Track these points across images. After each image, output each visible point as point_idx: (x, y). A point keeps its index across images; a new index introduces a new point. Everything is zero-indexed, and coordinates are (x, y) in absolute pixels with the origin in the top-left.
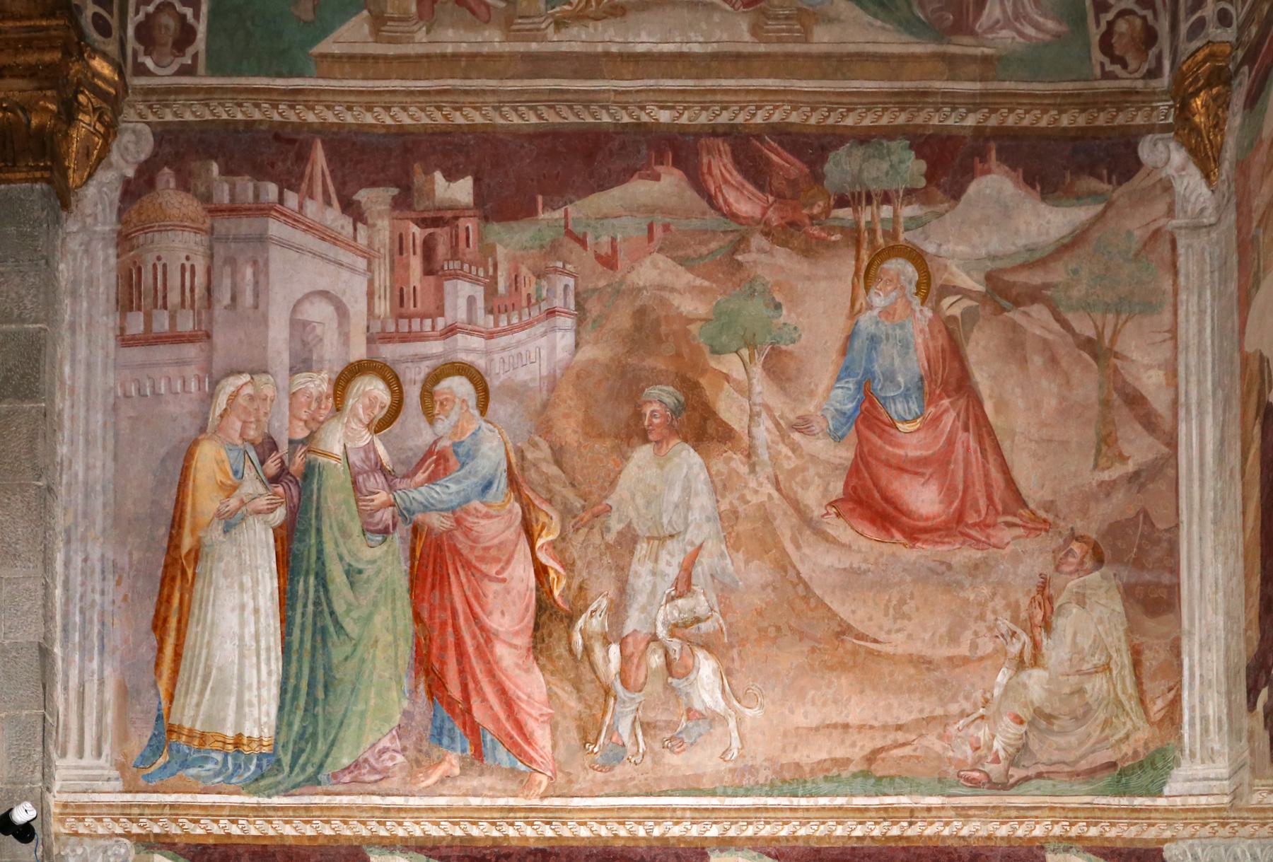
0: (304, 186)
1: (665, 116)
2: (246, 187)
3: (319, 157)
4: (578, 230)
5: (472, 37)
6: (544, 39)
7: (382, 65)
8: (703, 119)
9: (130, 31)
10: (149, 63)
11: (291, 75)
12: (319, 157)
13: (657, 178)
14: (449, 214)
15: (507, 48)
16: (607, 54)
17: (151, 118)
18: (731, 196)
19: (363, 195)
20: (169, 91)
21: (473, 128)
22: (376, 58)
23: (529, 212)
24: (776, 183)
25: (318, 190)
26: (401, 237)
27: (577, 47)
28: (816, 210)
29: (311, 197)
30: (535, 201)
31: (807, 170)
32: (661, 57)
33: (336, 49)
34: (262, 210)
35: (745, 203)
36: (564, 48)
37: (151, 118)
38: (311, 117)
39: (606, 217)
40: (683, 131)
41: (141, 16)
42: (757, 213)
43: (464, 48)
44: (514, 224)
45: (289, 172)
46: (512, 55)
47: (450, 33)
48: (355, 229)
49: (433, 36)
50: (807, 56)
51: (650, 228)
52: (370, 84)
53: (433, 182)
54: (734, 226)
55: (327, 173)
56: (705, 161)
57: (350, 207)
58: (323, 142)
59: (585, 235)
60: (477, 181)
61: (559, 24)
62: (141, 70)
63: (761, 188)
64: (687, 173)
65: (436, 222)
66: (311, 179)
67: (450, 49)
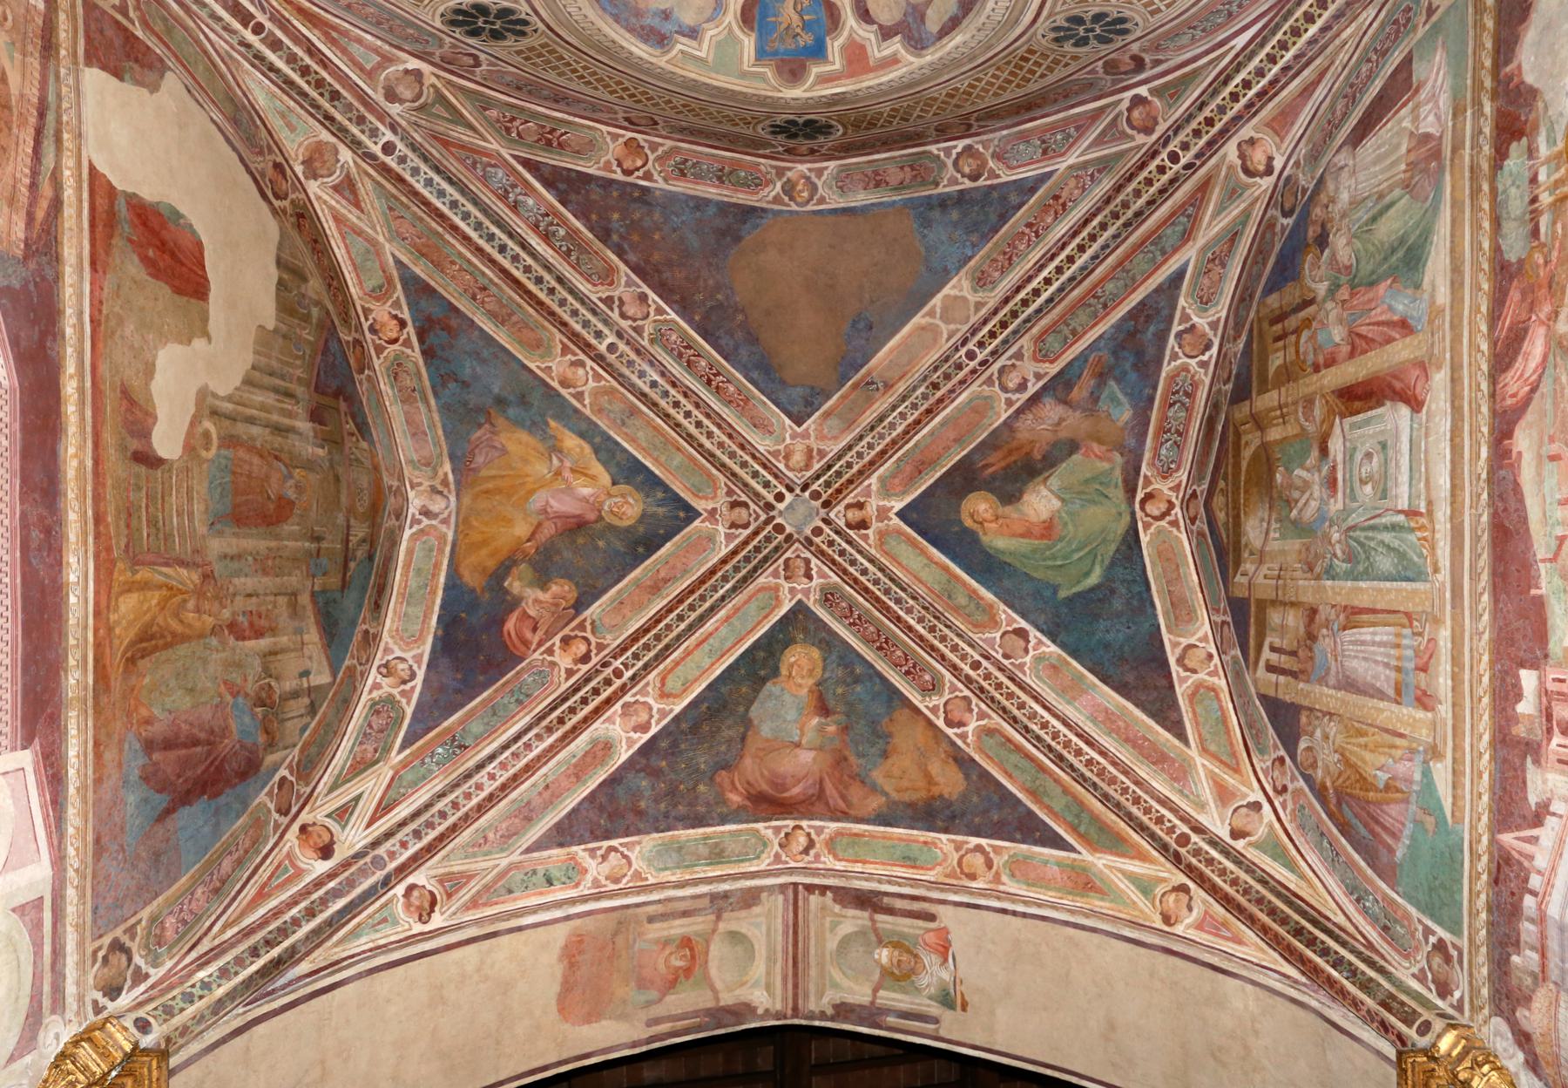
0: (1526, 864)
1: (1484, 452)
2: (1528, 930)
3: (1507, 838)
4: (1554, 544)
5: (1443, 658)
6: (1443, 584)
7: (1458, 755)
8: (1485, 409)
9: (1439, 1003)
10: (1457, 994)
11: (1462, 851)
12: (1507, 838)
13: (1520, 453)
14: (1544, 700)
15: (1449, 623)
16: (1452, 518)
17: (1486, 1011)
18: (1532, 365)
19: (1533, 799)
20: (1471, 983)
21: (1492, 663)
22: (1455, 760)
23: (1540, 604)
24: (1524, 316)
25: (1527, 848)
26: (1560, 761)
27: (1448, 549)
28: (1541, 261)
29: (1531, 858)
30: (1534, 597)
31: (1515, 282)
32: (1453, 462)
33: (1450, 800)
34: (1541, 920)
35: (1536, 346)
36: (1448, 564)
37: (1486, 1011)
38: (1485, 840)
39: (1544, 514)
40: (1492, 430)
41: (1433, 987)
42: (1542, 331)
43: (1449, 668)
44: (1549, 623)
45: (1517, 876)
46: (1453, 619)
47: (1441, 680)
48: (1554, 814)
49: (1442, 698)
50: (1452, 308)
51: (1553, 458)
52: (1468, 770)
53: (1524, 715)
54: (1551, 357)
55: (1517, 834)
56: (1509, 402)
57: (1537, 819)
58: (1499, 832)
59: (1557, 538)
60: (1522, 665)
61: (1436, 570)
62: (1459, 1007)
63: (1526, 330)
64: (1515, 422)
65: (1549, 717)
66: (1520, 853)
67: (1449, 682)
